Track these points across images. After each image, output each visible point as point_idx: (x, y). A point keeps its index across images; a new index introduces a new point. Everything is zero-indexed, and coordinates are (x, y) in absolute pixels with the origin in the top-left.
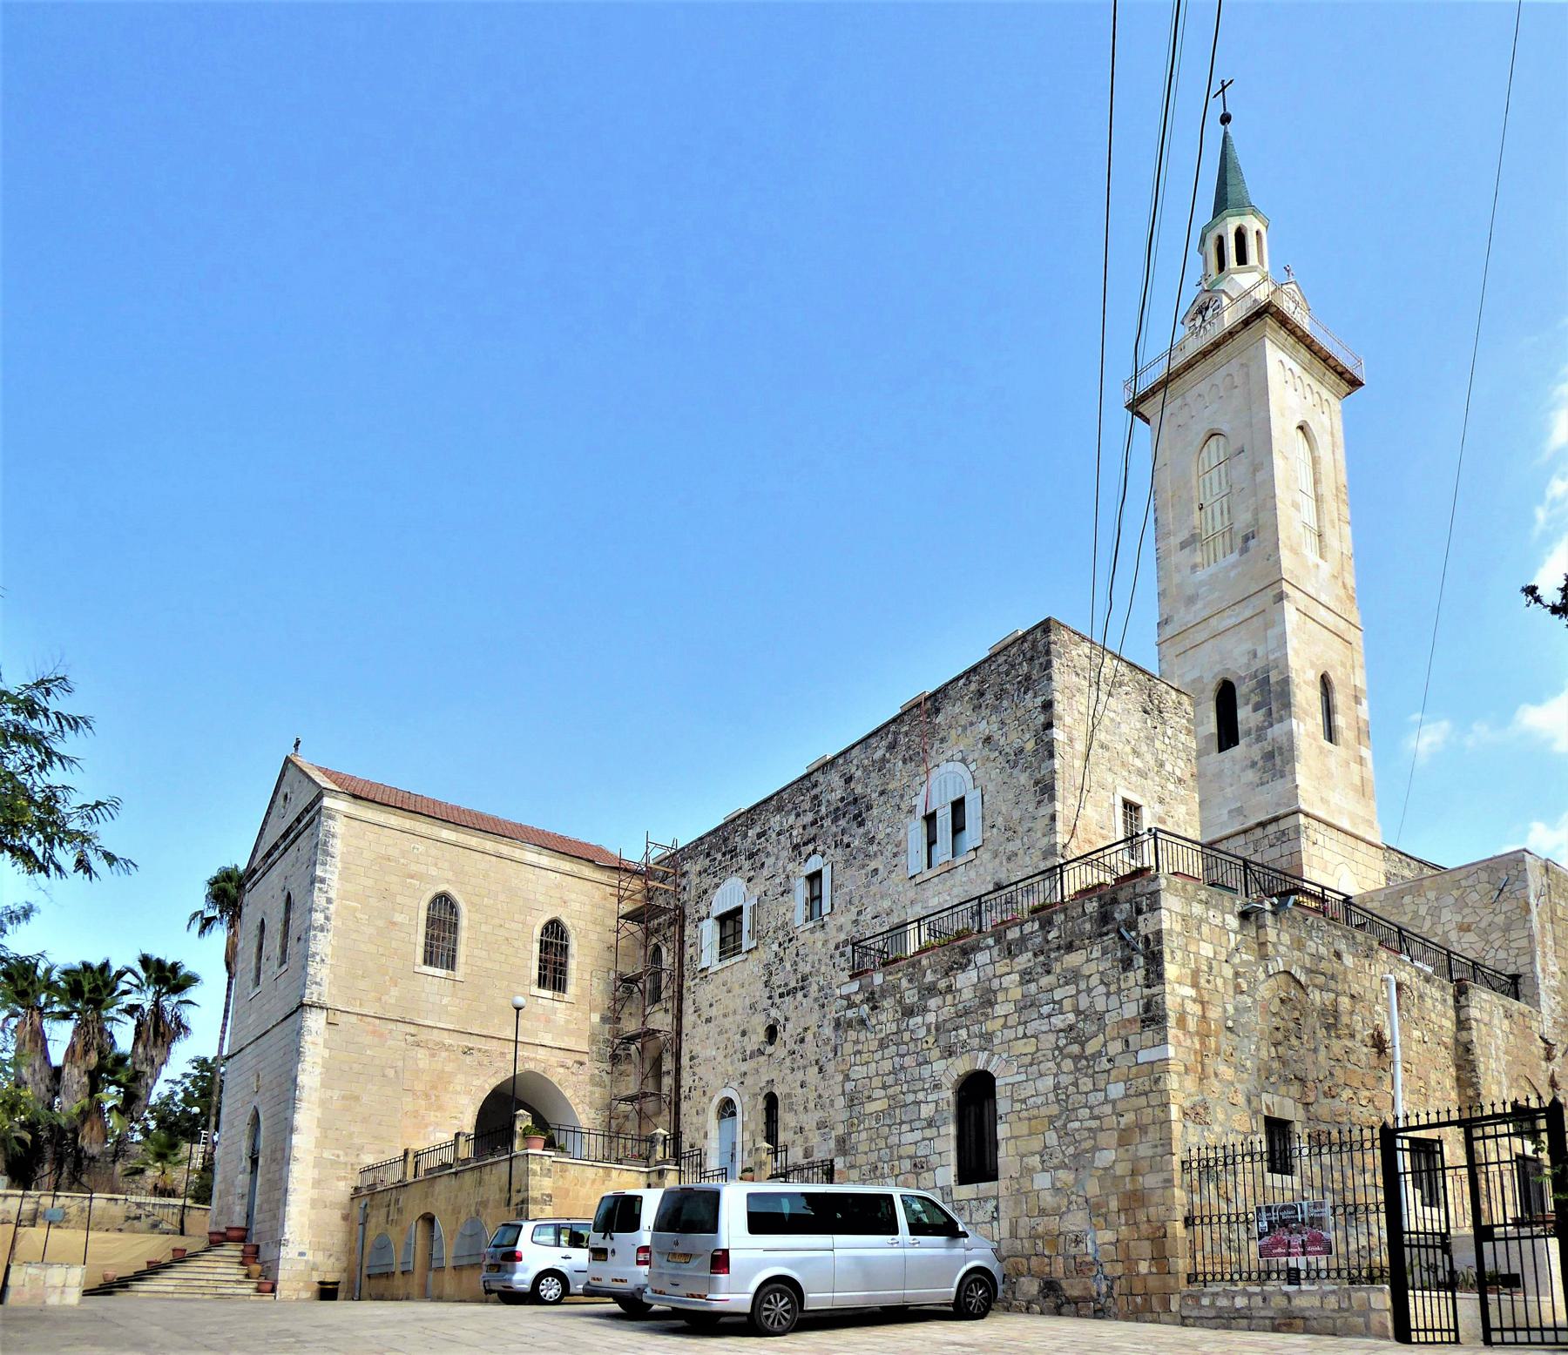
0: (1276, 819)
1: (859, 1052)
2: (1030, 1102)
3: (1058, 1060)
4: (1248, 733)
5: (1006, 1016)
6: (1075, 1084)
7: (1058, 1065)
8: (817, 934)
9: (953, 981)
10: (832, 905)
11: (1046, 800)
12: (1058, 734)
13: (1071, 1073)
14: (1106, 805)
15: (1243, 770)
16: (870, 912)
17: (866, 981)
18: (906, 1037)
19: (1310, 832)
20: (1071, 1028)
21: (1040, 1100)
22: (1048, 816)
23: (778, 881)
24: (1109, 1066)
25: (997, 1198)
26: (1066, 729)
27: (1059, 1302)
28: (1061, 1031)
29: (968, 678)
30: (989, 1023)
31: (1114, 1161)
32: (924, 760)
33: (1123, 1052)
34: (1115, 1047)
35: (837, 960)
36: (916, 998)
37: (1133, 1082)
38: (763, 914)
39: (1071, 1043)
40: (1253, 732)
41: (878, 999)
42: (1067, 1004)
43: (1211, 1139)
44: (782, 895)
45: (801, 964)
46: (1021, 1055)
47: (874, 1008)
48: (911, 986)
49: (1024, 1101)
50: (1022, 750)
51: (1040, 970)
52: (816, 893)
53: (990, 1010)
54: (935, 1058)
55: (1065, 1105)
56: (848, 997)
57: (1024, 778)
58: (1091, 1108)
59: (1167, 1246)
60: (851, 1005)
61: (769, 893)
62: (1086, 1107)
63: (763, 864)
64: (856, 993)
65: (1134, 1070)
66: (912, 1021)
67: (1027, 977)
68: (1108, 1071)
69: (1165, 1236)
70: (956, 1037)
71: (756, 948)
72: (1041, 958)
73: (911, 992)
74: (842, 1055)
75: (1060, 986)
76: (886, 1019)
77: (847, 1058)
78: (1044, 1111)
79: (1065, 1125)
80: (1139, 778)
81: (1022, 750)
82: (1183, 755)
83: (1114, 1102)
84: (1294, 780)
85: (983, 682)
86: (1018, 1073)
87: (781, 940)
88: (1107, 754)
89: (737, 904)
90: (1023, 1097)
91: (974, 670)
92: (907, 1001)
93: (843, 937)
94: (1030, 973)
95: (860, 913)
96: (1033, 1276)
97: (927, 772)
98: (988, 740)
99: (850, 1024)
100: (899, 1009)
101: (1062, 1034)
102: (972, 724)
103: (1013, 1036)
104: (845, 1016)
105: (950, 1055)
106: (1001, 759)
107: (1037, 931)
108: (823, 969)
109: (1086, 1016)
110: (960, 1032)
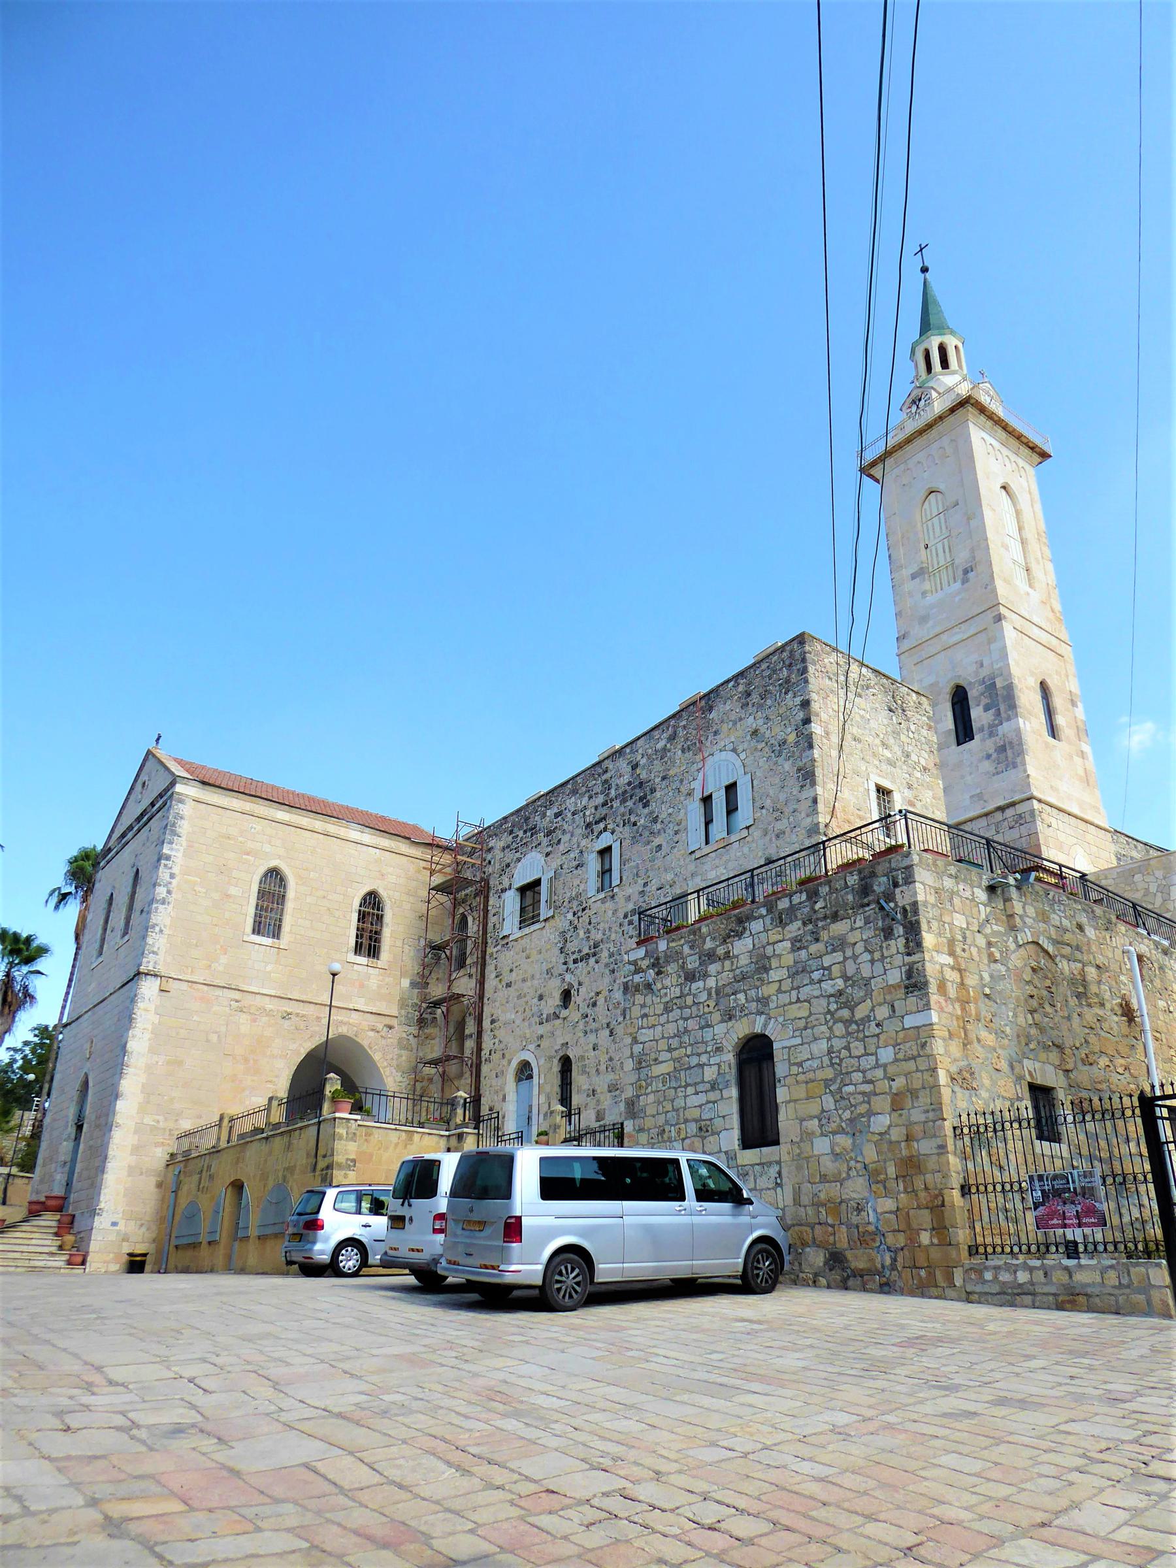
0: (1013, 804)
1: (645, 1015)
2: (807, 1065)
3: (830, 1024)
4: (981, 730)
5: (780, 981)
6: (847, 1048)
7: (830, 1029)
8: (607, 904)
9: (731, 948)
10: (621, 878)
11: (808, 786)
12: (816, 728)
13: (843, 1037)
14: (861, 789)
15: (980, 761)
16: (652, 887)
17: (651, 947)
18: (689, 1000)
19: (1044, 816)
20: (840, 993)
21: (815, 1064)
22: (810, 800)
23: (572, 855)
24: (877, 1031)
25: (779, 1163)
26: (823, 724)
27: (845, 1275)
28: (832, 995)
29: (736, 682)
30: (764, 987)
31: (889, 1127)
32: (700, 750)
33: (890, 1017)
34: (882, 1012)
35: (626, 928)
36: (697, 963)
37: (901, 1046)
38: (559, 885)
39: (841, 1008)
40: (986, 728)
41: (664, 965)
42: (836, 970)
43: (980, 1105)
44: (576, 868)
45: (593, 931)
46: (795, 1018)
47: (659, 973)
48: (692, 952)
49: (800, 1064)
50: (785, 742)
51: (809, 938)
52: (607, 867)
53: (765, 975)
54: (716, 1022)
55: (839, 1068)
56: (635, 963)
57: (787, 766)
58: (864, 1072)
59: (946, 1215)
60: (638, 971)
61: (565, 866)
62: (859, 1070)
63: (559, 841)
64: (643, 959)
65: (901, 1035)
66: (694, 986)
67: (798, 945)
68: (877, 1035)
69: (943, 1205)
70: (735, 1000)
71: (553, 917)
72: (810, 927)
73: (693, 958)
74: (631, 1018)
75: (827, 953)
76: (671, 983)
77: (635, 1021)
78: (820, 1075)
79: (840, 1089)
80: (889, 767)
81: (785, 742)
82: (926, 747)
83: (885, 1066)
84: (1025, 771)
85: (749, 684)
86: (793, 1037)
87: (575, 909)
88: (859, 746)
89: (536, 877)
90: (799, 1060)
91: (741, 674)
92: (690, 966)
93: (631, 906)
94: (800, 941)
95: (645, 884)
96: (818, 1246)
97: (704, 759)
98: (755, 732)
99: (637, 989)
100: (682, 974)
101: (832, 999)
102: (741, 719)
103: (787, 1001)
104: (632, 980)
105: (730, 1019)
106: (767, 749)
107: (803, 902)
108: (613, 937)
109: (854, 982)
110: (738, 996)
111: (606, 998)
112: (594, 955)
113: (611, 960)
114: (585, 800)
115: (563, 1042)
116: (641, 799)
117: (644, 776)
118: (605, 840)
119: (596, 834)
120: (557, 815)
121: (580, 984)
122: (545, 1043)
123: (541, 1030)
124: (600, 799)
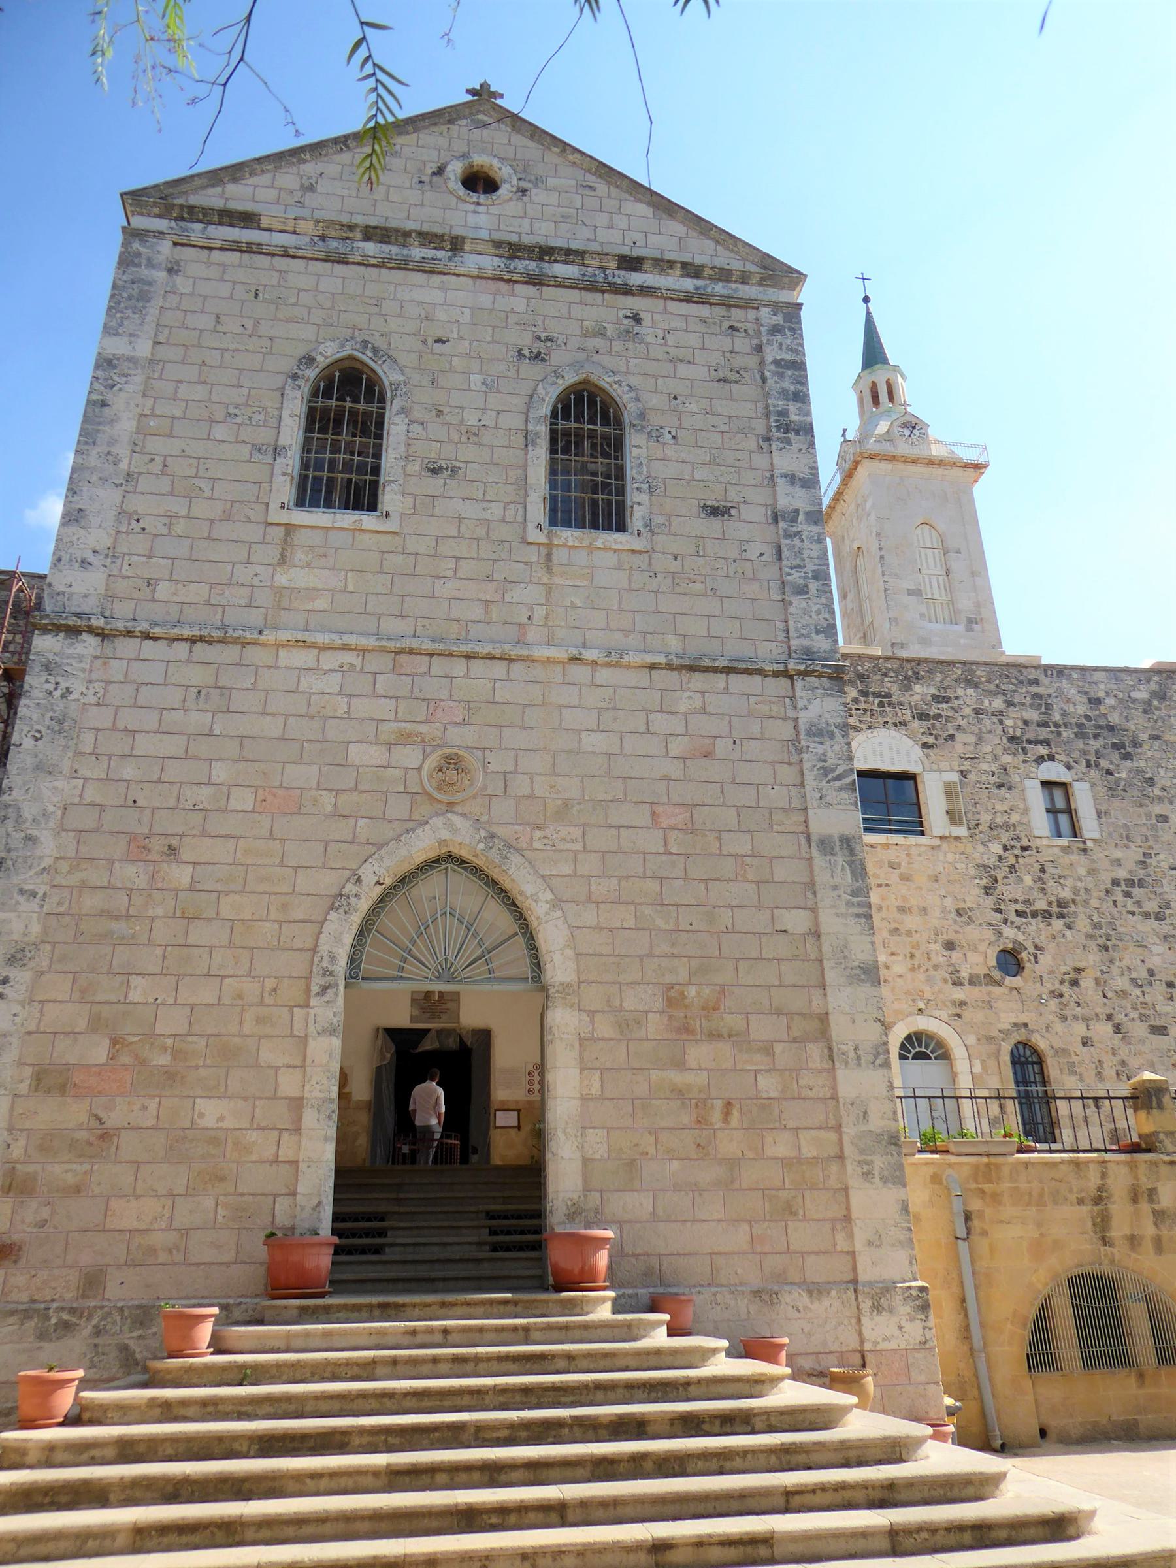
23: (984, 766)
63: (951, 737)
71: (957, 838)
93: (1122, 874)
108: (1094, 902)
111: (1097, 981)
112: (1061, 916)
113: (1098, 932)
114: (998, 703)
115: (1013, 1020)
116: (1115, 746)
117: (1114, 719)
118: (1054, 771)
119: (1031, 757)
120: (936, 699)
121: (1036, 947)
122: (967, 1014)
123: (959, 994)
124: (1034, 715)
